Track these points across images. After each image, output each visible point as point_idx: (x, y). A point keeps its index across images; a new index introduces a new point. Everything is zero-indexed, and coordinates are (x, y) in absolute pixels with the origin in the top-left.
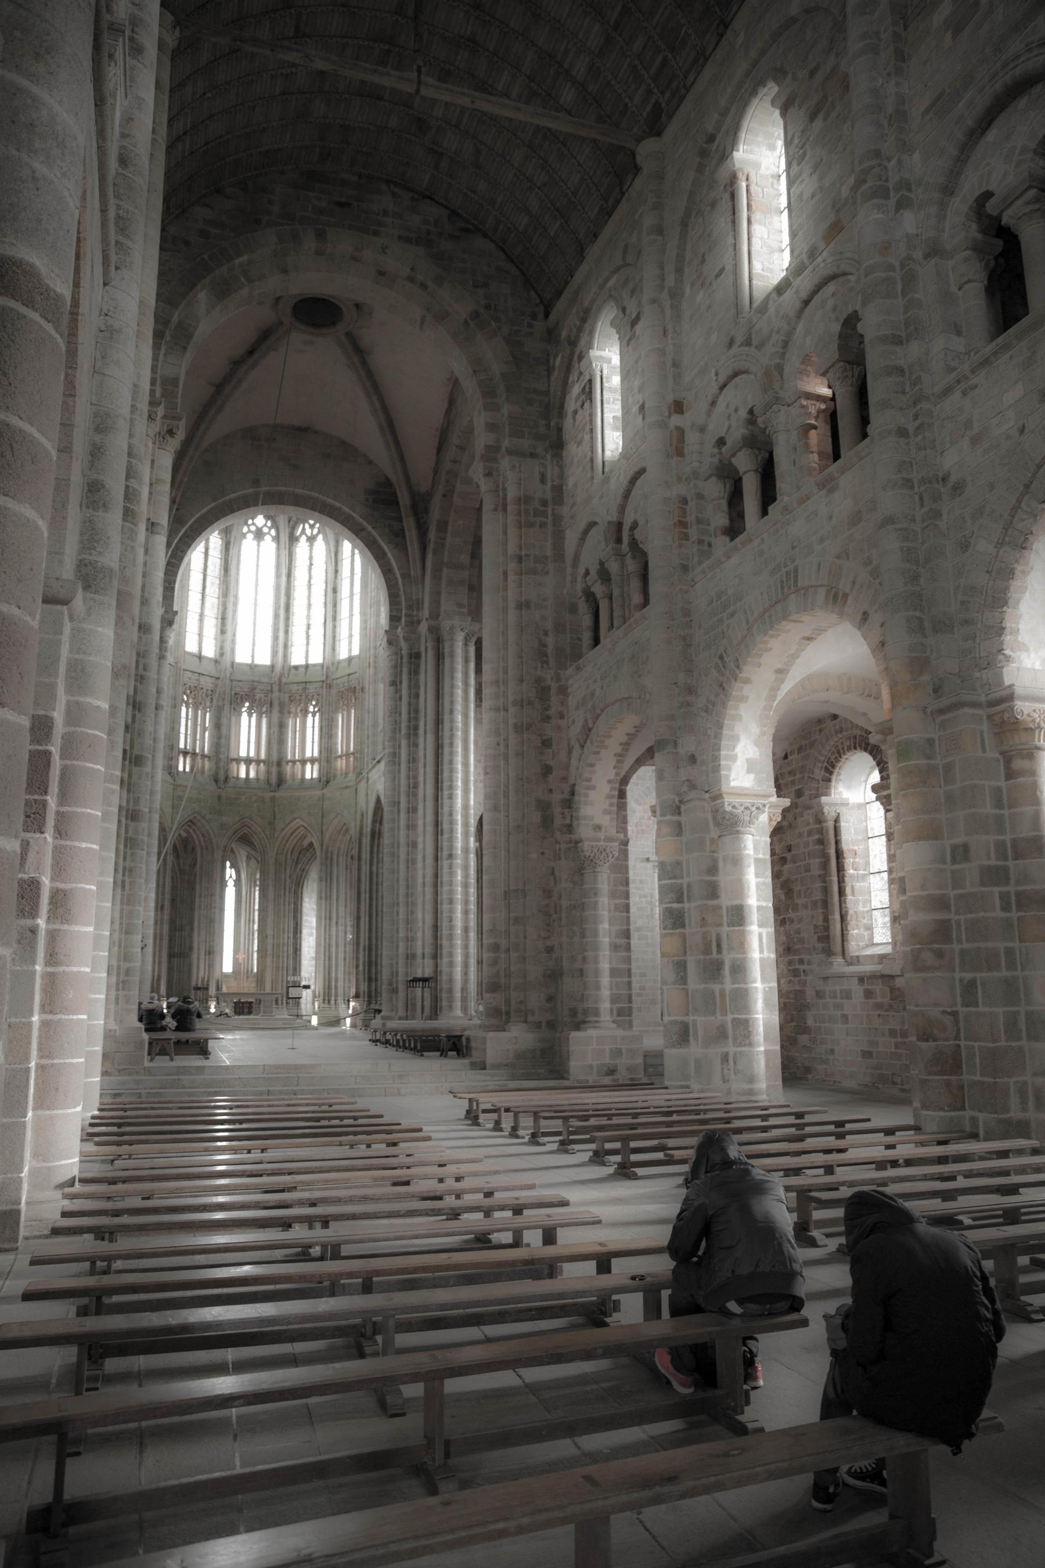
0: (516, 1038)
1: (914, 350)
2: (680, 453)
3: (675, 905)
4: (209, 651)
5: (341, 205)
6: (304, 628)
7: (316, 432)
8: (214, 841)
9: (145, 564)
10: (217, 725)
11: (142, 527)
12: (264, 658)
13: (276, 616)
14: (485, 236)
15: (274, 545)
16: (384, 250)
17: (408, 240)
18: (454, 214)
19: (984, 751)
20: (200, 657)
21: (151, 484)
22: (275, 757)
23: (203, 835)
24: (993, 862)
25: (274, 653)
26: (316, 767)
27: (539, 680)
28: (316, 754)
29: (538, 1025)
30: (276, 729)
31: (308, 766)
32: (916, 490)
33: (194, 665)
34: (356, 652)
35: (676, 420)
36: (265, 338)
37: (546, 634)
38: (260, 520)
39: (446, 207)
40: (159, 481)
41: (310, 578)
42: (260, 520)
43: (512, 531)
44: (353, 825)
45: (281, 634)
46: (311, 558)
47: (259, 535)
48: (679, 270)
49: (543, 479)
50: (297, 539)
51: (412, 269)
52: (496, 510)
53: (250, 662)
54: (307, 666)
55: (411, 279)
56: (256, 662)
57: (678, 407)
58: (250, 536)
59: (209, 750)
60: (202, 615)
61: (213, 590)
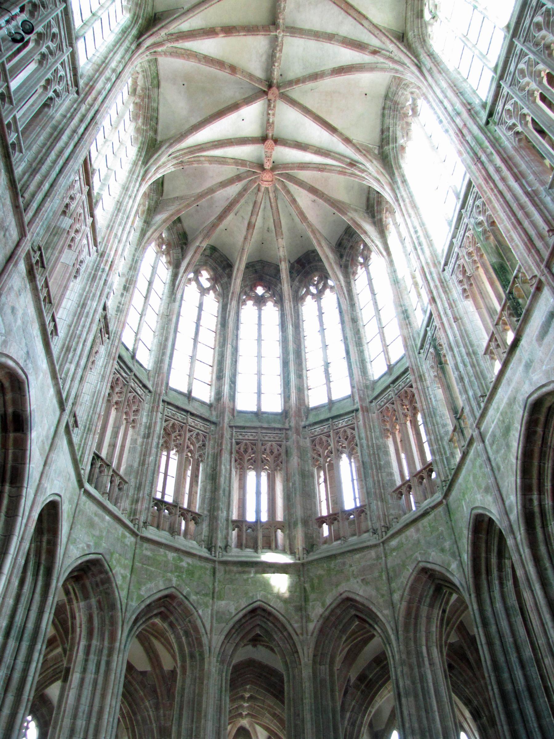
6: (323, 369)
8: (205, 640)
10: (213, 476)
12: (273, 404)
13: (285, 364)
20: (189, 396)
22: (299, 512)
23: (187, 634)
25: (287, 398)
33: (181, 402)
34: (397, 352)
42: (260, 290)
44: (454, 566)
45: (293, 377)
46: (320, 309)
50: (302, 299)
53: (255, 409)
54: (331, 403)
56: (263, 409)
58: (250, 303)
59: (200, 508)
61: (208, 337)
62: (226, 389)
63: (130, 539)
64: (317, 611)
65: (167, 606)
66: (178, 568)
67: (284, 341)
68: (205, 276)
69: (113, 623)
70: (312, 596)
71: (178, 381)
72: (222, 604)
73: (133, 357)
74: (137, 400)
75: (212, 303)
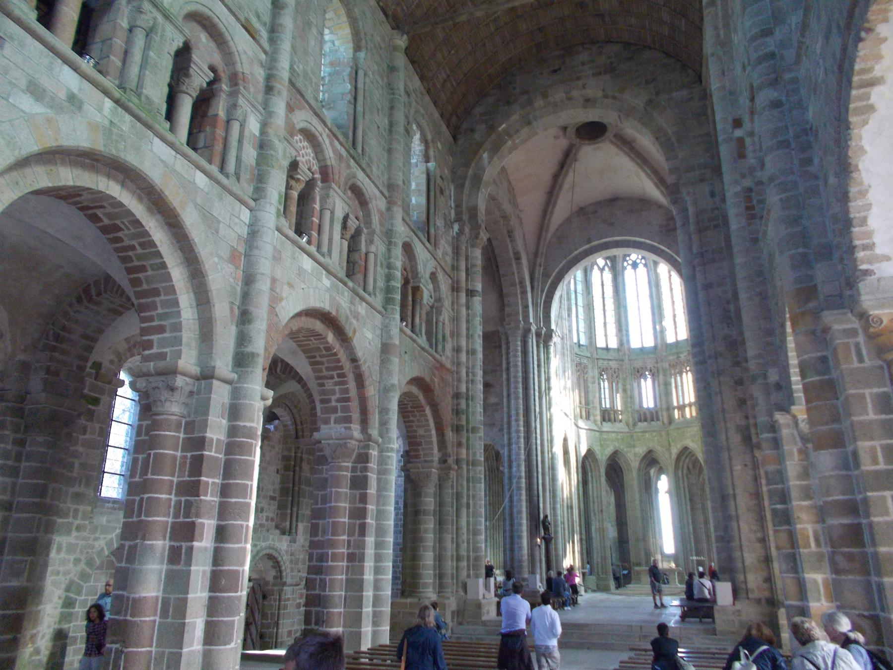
0: (739, 611)
1: (778, 34)
2: (742, 155)
3: (779, 506)
4: (613, 344)
5: (555, 71)
7: (623, 199)
9: (468, 315)
11: (463, 295)
12: (649, 343)
14: (650, 48)
15: (645, 269)
16: (584, 87)
17: (600, 74)
18: (627, 45)
19: (861, 360)
21: (467, 270)
24: (882, 466)
25: (655, 337)
26: (693, 408)
27: (726, 337)
28: (693, 400)
29: (759, 601)
30: (662, 387)
31: (687, 410)
32: (793, 146)
33: (604, 355)
35: (738, 133)
36: (567, 159)
37: (728, 303)
38: (634, 257)
39: (621, 42)
40: (474, 266)
41: (671, 284)
43: (695, 238)
47: (635, 265)
48: (727, 26)
49: (713, 195)
51: (603, 90)
52: (684, 225)
53: (640, 346)
55: (606, 96)
57: (737, 123)
58: (629, 267)
60: (605, 324)
62: (625, 338)
63: (598, 434)
64: (675, 451)
65: (615, 454)
66: (617, 439)
67: (651, 296)
68: (601, 262)
69: (598, 466)
70: (672, 444)
71: (601, 343)
72: (637, 450)
73: (579, 345)
74: (585, 367)
75: (608, 276)
